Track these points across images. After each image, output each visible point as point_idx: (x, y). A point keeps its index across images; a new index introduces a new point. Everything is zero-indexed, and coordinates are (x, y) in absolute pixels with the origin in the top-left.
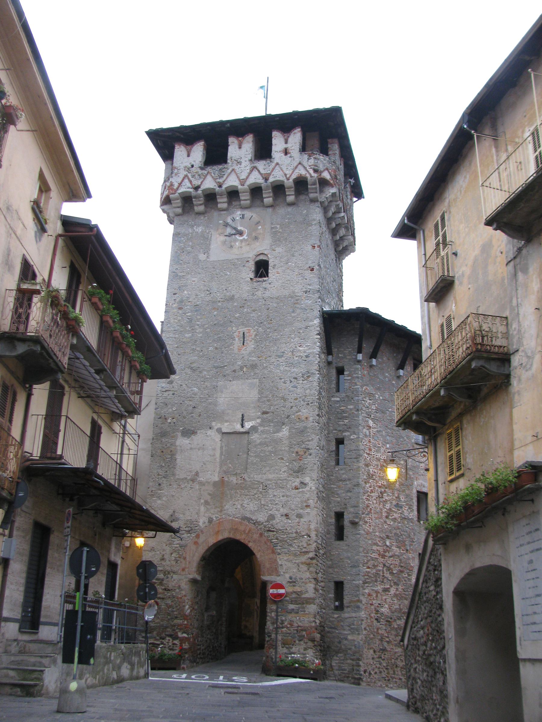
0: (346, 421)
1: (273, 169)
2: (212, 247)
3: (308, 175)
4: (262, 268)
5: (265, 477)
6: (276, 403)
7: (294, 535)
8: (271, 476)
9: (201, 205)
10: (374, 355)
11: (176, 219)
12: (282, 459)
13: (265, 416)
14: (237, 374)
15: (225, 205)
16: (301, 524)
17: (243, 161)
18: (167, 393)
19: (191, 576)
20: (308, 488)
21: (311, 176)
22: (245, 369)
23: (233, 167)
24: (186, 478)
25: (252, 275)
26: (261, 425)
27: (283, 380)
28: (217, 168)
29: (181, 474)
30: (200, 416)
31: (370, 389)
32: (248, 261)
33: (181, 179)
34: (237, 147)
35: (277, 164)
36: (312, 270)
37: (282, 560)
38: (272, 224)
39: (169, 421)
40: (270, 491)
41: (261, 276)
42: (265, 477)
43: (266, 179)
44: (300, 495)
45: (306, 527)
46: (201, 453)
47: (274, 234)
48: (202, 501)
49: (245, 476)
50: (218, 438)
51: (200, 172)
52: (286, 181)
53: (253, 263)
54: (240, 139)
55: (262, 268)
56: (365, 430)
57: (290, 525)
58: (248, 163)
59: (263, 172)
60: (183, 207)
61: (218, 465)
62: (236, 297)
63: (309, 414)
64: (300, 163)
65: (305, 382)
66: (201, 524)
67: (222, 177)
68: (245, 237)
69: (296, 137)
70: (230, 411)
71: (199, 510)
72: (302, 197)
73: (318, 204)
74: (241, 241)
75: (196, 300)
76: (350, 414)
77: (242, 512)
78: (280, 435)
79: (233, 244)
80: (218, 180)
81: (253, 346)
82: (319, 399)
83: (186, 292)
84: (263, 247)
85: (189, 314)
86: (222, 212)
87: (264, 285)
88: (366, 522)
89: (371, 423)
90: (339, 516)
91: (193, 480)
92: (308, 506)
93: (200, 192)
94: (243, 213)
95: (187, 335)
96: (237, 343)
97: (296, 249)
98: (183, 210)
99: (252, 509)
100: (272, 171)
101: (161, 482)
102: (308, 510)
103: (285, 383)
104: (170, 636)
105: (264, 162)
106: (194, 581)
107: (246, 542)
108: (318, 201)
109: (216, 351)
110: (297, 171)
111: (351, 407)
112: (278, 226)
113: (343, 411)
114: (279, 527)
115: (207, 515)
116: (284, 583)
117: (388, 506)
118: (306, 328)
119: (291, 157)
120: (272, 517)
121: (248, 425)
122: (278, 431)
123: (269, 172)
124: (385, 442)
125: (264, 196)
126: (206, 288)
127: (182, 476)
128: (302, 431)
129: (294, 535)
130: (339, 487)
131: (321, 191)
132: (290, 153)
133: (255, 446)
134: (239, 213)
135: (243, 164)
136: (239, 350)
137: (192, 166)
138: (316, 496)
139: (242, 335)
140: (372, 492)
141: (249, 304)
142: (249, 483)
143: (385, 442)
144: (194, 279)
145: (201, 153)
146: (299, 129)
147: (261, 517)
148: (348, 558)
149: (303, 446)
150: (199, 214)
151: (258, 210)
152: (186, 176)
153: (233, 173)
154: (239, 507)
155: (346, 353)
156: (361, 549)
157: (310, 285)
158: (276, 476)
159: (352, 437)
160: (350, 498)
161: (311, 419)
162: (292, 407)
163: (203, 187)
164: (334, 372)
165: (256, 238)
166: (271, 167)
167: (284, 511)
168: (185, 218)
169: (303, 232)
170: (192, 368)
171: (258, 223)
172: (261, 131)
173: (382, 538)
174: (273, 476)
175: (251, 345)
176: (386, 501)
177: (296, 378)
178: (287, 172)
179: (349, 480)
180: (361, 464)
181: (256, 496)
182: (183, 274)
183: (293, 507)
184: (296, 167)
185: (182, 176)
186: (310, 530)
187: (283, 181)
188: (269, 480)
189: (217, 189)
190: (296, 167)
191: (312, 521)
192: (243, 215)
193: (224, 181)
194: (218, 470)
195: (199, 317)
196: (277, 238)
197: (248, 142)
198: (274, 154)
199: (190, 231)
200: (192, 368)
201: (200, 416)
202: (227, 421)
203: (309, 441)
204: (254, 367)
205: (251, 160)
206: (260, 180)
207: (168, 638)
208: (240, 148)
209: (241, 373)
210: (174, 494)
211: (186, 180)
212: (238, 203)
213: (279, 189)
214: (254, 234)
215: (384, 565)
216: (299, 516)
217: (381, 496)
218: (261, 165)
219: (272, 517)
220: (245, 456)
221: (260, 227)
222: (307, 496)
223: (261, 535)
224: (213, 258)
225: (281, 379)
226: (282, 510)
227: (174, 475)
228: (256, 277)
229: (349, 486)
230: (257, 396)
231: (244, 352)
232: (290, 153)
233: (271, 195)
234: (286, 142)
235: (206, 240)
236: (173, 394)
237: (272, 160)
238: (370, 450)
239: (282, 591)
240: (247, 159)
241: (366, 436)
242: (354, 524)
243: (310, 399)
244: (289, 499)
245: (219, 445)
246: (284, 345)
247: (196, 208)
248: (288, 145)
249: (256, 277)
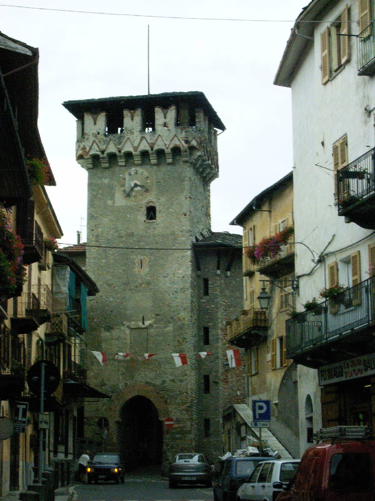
1: (157, 139)
3: (181, 146)
4: (151, 212)
12: (169, 345)
13: (157, 317)
15: (123, 164)
19: (115, 420)
21: (184, 146)
22: (143, 286)
23: (128, 136)
25: (144, 218)
27: (168, 293)
34: (130, 119)
35: (159, 135)
37: (171, 408)
41: (151, 219)
50: (128, 332)
53: (145, 208)
54: (132, 111)
55: (151, 212)
63: (185, 315)
64: (175, 136)
65: (182, 294)
67: (121, 144)
78: (167, 329)
80: (118, 146)
81: (148, 269)
83: (100, 229)
86: (122, 168)
92: (186, 375)
94: (137, 169)
106: (118, 423)
110: (173, 142)
120: (164, 382)
121: (147, 323)
122: (166, 327)
123: (154, 142)
125: (151, 158)
128: (181, 328)
137: (99, 133)
145: (104, 119)
147: (158, 382)
152: (94, 141)
153: (128, 140)
166: (155, 138)
167: (172, 378)
175: (146, 269)
177: (176, 292)
178: (166, 143)
181: (154, 369)
184: (173, 138)
185: (91, 141)
186: (187, 389)
190: (173, 138)
197: (138, 115)
203: (186, 333)
204: (149, 283)
206: (148, 148)
213: (160, 153)
216: (181, 381)
234: (165, 117)
248: (167, 120)
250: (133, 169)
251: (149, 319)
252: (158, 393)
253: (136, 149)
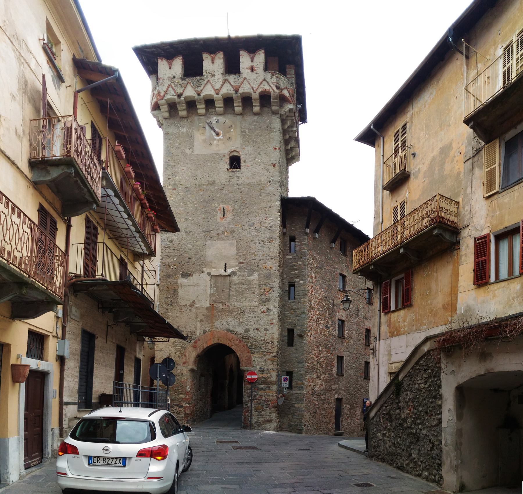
0: (296, 272)
1: (242, 83)
5: (242, 304)
6: (249, 257)
7: (263, 341)
8: (246, 304)
9: (184, 110)
10: (317, 231)
11: (165, 123)
13: (241, 265)
14: (220, 236)
16: (267, 335)
17: (216, 74)
18: (169, 249)
20: (272, 313)
22: (226, 233)
24: (186, 305)
26: (238, 271)
28: (195, 79)
29: (182, 302)
30: (194, 264)
31: (313, 253)
32: (224, 156)
33: (166, 88)
35: (245, 79)
36: (274, 166)
38: (242, 128)
39: (172, 267)
40: (246, 314)
41: (234, 168)
42: (242, 304)
43: (237, 91)
44: (267, 316)
45: (271, 337)
46: (196, 290)
47: (244, 136)
48: (198, 319)
49: (229, 304)
50: (208, 278)
51: (181, 82)
52: (253, 93)
56: (309, 279)
57: (260, 335)
58: (220, 76)
59: (233, 84)
60: (170, 112)
61: (209, 296)
62: (216, 182)
64: (264, 80)
66: (198, 334)
67: (200, 87)
68: (221, 137)
69: (260, 58)
70: (216, 261)
71: (197, 325)
72: (266, 109)
73: (279, 116)
74: (218, 140)
75: (186, 183)
76: (299, 268)
77: (227, 327)
79: (212, 142)
80: (197, 89)
82: (279, 256)
84: (235, 145)
85: (182, 194)
87: (238, 174)
88: (308, 336)
89: (313, 275)
90: (291, 332)
91: (191, 306)
92: (272, 324)
93: (182, 98)
95: (181, 209)
96: (219, 215)
97: (261, 149)
98: (170, 114)
99: (234, 325)
100: (241, 84)
101: (168, 307)
102: (272, 326)
103: (255, 243)
105: (234, 76)
107: (230, 346)
108: (278, 113)
109: (204, 220)
110: (262, 86)
111: (300, 263)
112: (247, 131)
113: (294, 265)
114: (252, 336)
115: (202, 328)
116: (256, 372)
117: (321, 326)
118: (270, 207)
119: (256, 74)
121: (229, 271)
122: (251, 275)
124: (321, 288)
125: (235, 105)
126: (193, 175)
127: (183, 303)
128: (268, 276)
129: (263, 341)
130: (290, 313)
131: (281, 106)
132: (255, 70)
133: (235, 284)
134: (215, 118)
135: (217, 77)
136: (221, 220)
138: (277, 317)
139: (223, 210)
140: (312, 317)
141: (227, 187)
142: (231, 308)
143: (321, 288)
144: (183, 168)
146: (263, 51)
147: (240, 330)
148: (296, 357)
149: (269, 285)
151: (230, 116)
153: (208, 83)
154: (225, 323)
155: (297, 228)
156: (305, 352)
157: (272, 176)
158: (249, 304)
159: (300, 282)
160: (298, 320)
161: (274, 268)
162: (260, 260)
163: (184, 95)
164: (288, 239)
165: (229, 138)
168: (172, 121)
169: (267, 137)
170: (186, 232)
172: (231, 51)
173: (317, 346)
174: (248, 304)
175: (229, 217)
176: (320, 324)
179: (298, 309)
180: (306, 300)
182: (174, 164)
183: (262, 324)
184: (261, 83)
186: (273, 338)
187: (250, 94)
188: (245, 306)
189: (197, 97)
190: (261, 83)
191: (274, 332)
193: (202, 90)
194: (209, 299)
195: (189, 196)
196: (246, 139)
198: (242, 70)
199: (177, 131)
200: (186, 232)
201: (194, 264)
202: (214, 268)
203: (273, 282)
204: (233, 232)
205: (223, 74)
208: (213, 63)
209: (223, 236)
210: (178, 315)
212: (213, 110)
213: (247, 100)
215: (318, 362)
217: (317, 320)
218: (232, 78)
219: (247, 330)
220: (228, 291)
222: (271, 317)
223: (240, 341)
224: (196, 152)
225: (252, 241)
226: (254, 325)
227: (177, 303)
228: (231, 168)
229: (298, 313)
230: (235, 252)
231: (225, 222)
232: (255, 70)
233: (241, 104)
234: (252, 61)
235: (190, 137)
236: (174, 249)
237: (241, 75)
238: (312, 291)
239: (255, 377)
240: (220, 73)
241: (310, 282)
242: (301, 336)
243: (273, 255)
244: (259, 319)
245: (209, 283)
246: (254, 218)
247: (180, 112)
248: (255, 64)
249: (231, 168)
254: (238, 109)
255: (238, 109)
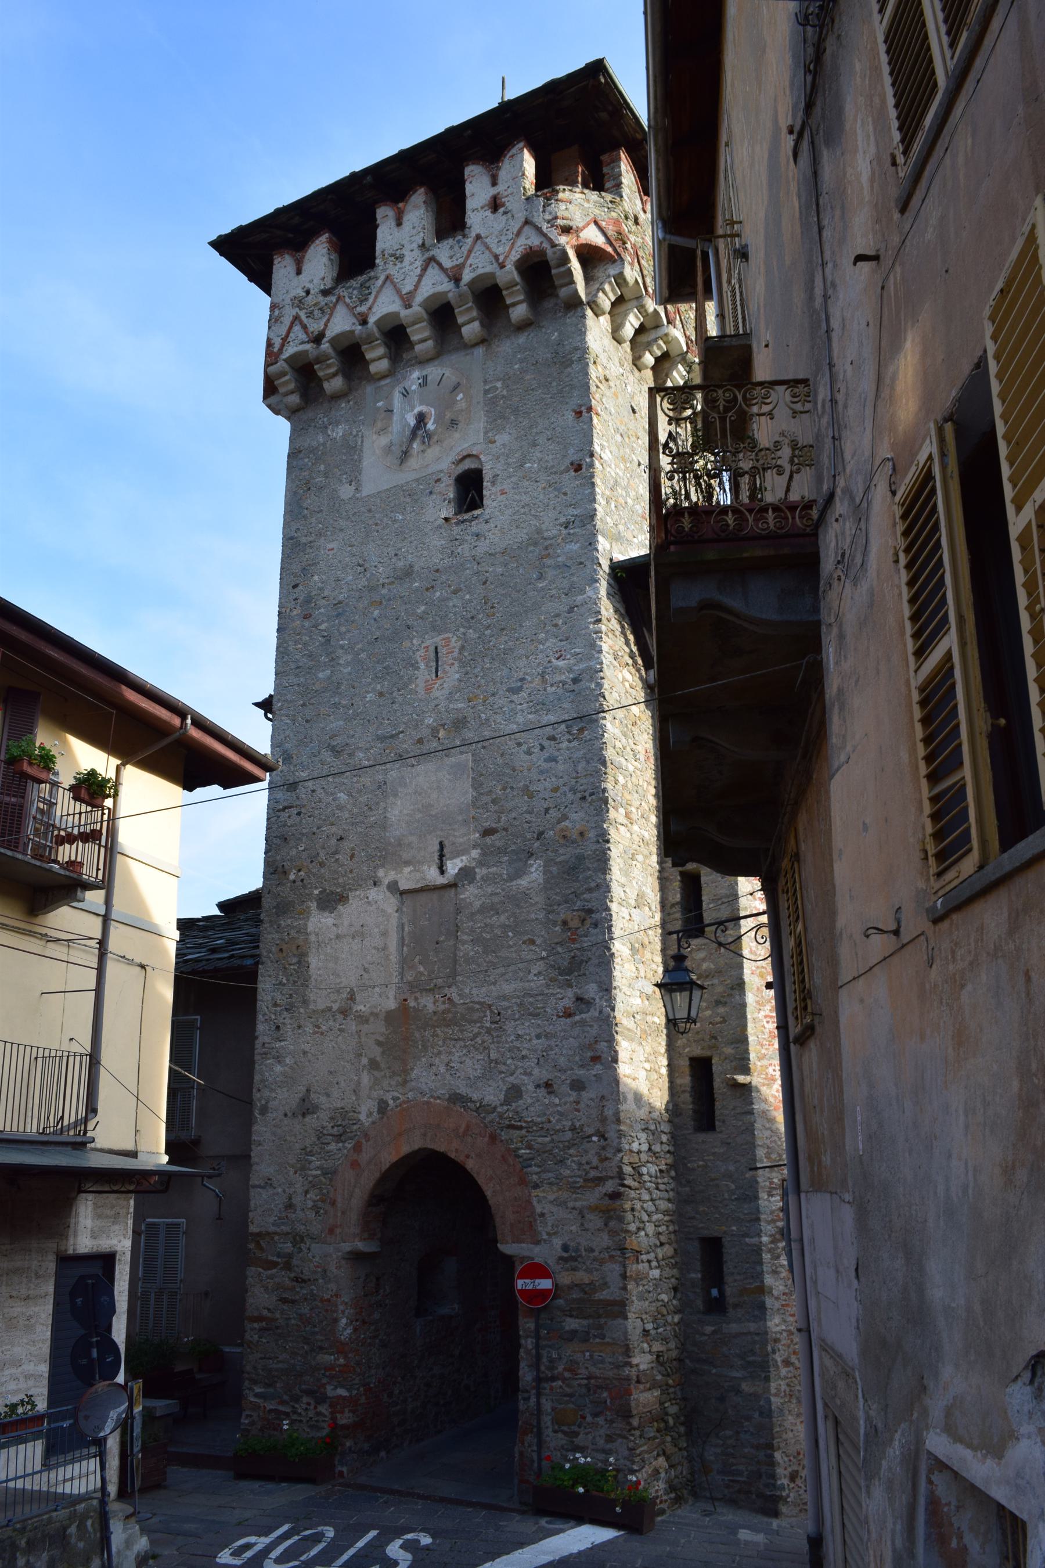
1: (470, 251)
2: (365, 463)
4: (470, 489)
7: (569, 1135)
8: (507, 988)
12: (532, 942)
13: (488, 840)
15: (383, 365)
16: (582, 1106)
19: (347, 1247)
22: (442, 734)
23: (388, 272)
24: (330, 1009)
25: (448, 511)
26: (481, 864)
27: (524, 747)
29: (319, 1000)
30: (352, 856)
32: (438, 480)
34: (393, 223)
35: (478, 237)
37: (544, 1201)
39: (292, 877)
40: (509, 1026)
43: (457, 280)
44: (576, 1031)
48: (365, 1061)
49: (453, 993)
50: (390, 903)
51: (323, 300)
53: (451, 481)
55: (470, 489)
58: (417, 253)
62: (416, 568)
64: (527, 222)
65: (575, 743)
66: (363, 1117)
67: (366, 299)
70: (413, 839)
71: (359, 1083)
78: (523, 882)
80: (359, 309)
81: (457, 676)
83: (316, 578)
86: (383, 383)
87: (474, 527)
91: (345, 1012)
93: (325, 346)
94: (424, 373)
96: (423, 673)
103: (529, 753)
104: (309, 1393)
105: (451, 241)
106: (356, 1257)
107: (460, 1158)
114: (532, 1115)
115: (375, 1094)
116: (552, 1264)
118: (571, 610)
119: (505, 213)
120: (514, 1093)
121: (453, 867)
122: (518, 874)
123: (461, 260)
125: (460, 320)
127: (321, 1005)
129: (569, 1135)
132: (503, 205)
136: (428, 690)
137: (308, 292)
139: (432, 655)
144: (330, 546)
145: (325, 260)
147: (492, 1094)
150: (336, 397)
152: (296, 318)
153: (388, 283)
154: (442, 1069)
162: (547, 810)
163: (329, 334)
166: (465, 249)
167: (541, 1074)
171: (456, 387)
172: (436, 170)
175: (452, 674)
177: (552, 738)
178: (499, 250)
181: (479, 1040)
183: (562, 1061)
188: (504, 998)
190: (518, 234)
192: (425, 378)
193: (370, 309)
195: (343, 629)
197: (416, 207)
201: (352, 856)
202: (407, 863)
203: (590, 890)
206: (446, 286)
207: (305, 1400)
208: (399, 224)
210: (306, 1047)
211: (297, 328)
214: (448, 416)
216: (578, 1085)
218: (446, 253)
221: (461, 396)
222: (594, 1031)
227: (305, 1002)
230: (471, 793)
231: (438, 694)
232: (503, 205)
233: (475, 313)
234: (494, 184)
239: (545, 1284)
240: (415, 246)
245: (394, 921)
250: (416, 374)
251: (457, 854)
252: (493, 1138)
253: (407, 301)
254: (471, 329)
255: (471, 329)
